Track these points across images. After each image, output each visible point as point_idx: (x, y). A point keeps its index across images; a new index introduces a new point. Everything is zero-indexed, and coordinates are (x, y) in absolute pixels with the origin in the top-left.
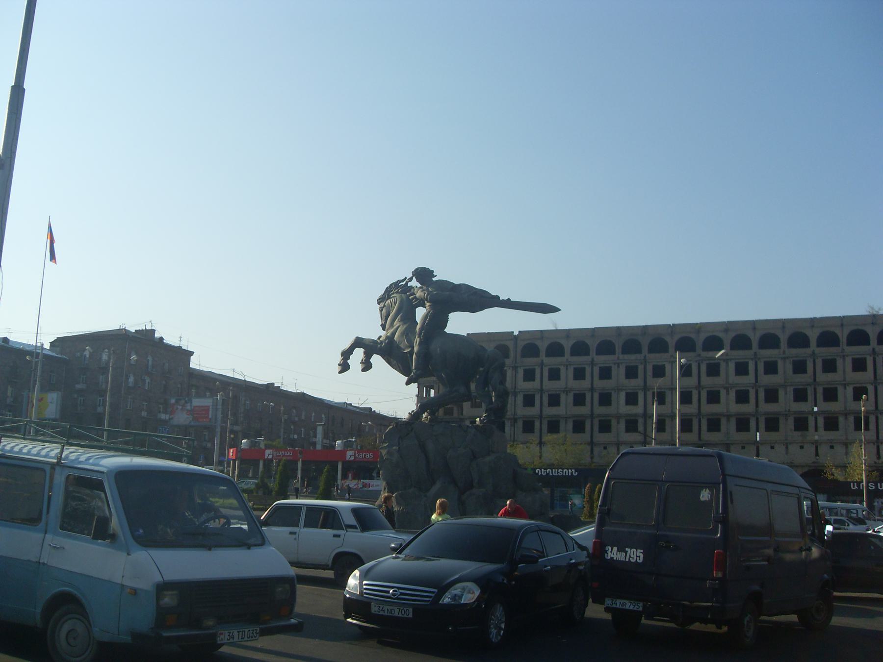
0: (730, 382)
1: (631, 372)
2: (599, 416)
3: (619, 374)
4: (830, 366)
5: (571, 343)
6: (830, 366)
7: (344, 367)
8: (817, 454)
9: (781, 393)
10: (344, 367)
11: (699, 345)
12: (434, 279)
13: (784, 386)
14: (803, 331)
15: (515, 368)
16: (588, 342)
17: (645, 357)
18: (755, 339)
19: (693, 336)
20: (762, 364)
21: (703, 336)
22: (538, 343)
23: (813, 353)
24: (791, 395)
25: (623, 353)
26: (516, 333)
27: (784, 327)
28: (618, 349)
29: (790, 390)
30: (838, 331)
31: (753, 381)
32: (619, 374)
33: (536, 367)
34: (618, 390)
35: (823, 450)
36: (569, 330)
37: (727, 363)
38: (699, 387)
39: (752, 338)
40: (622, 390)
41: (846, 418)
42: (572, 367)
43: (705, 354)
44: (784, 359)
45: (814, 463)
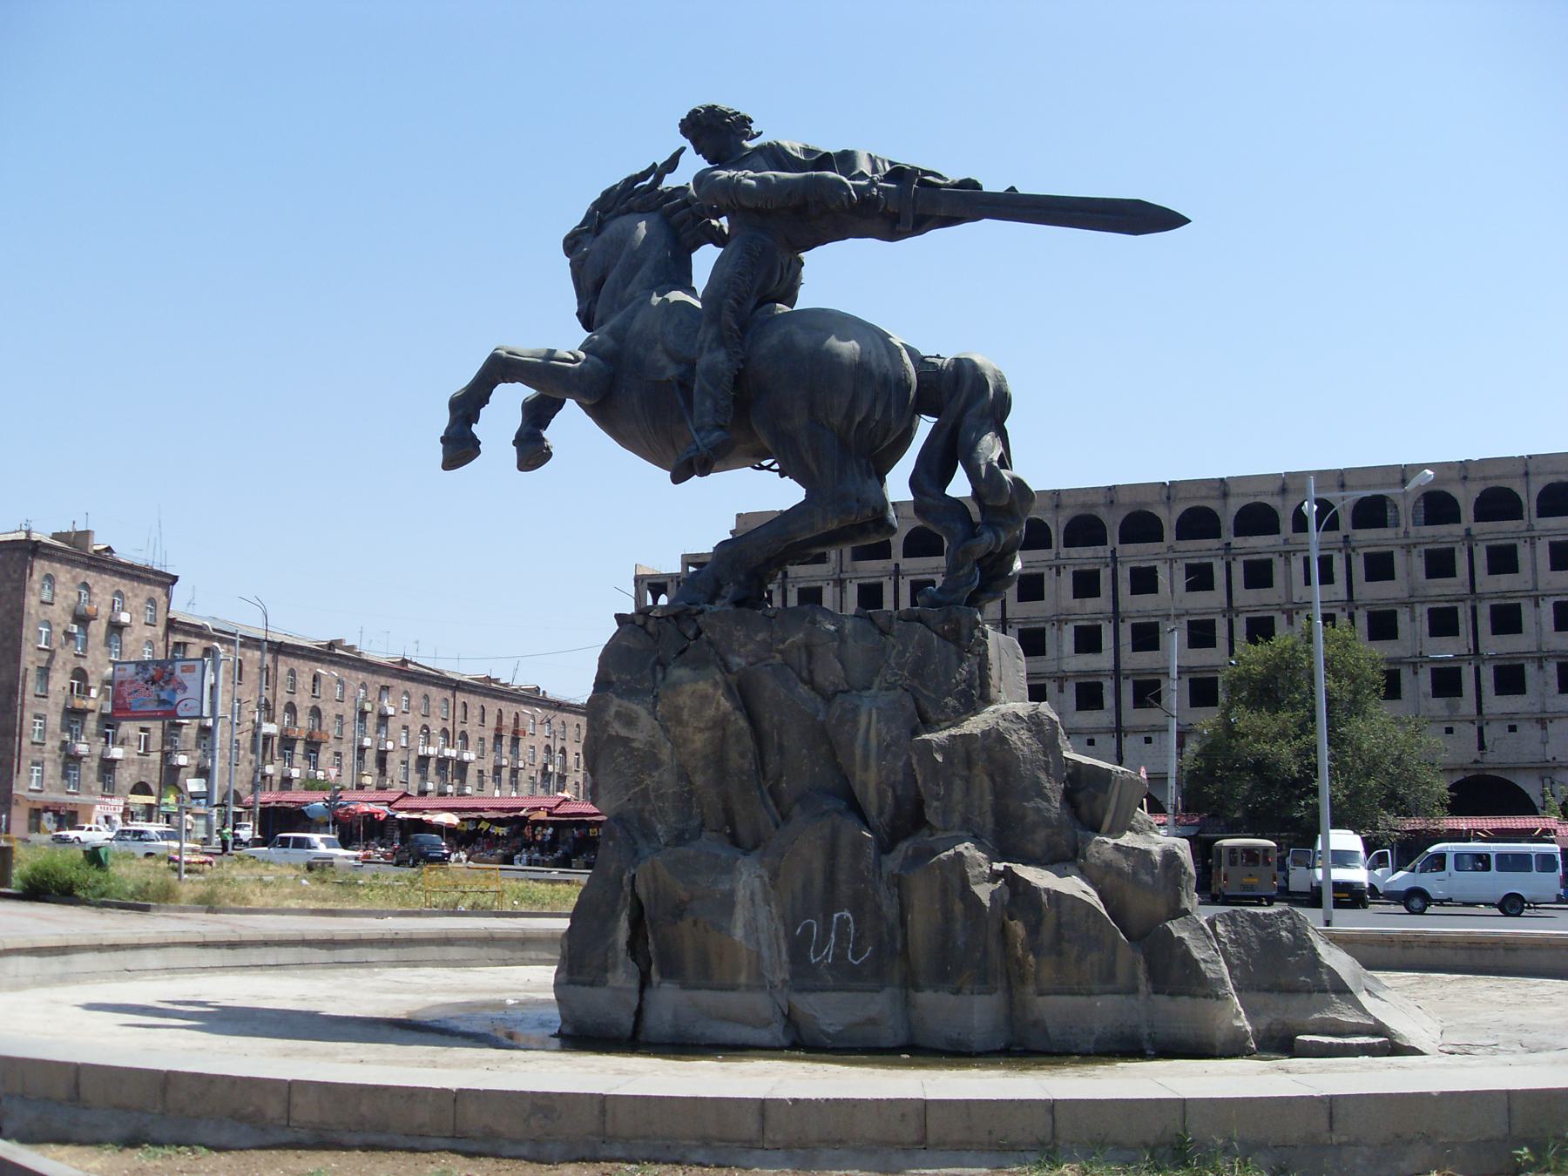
1: (1086, 584)
4: (1503, 560)
6: (1503, 560)
7: (460, 446)
8: (1482, 746)
9: (1403, 618)
10: (460, 446)
11: (1227, 523)
12: (750, 144)
13: (1409, 604)
14: (1447, 489)
15: (840, 583)
17: (1113, 552)
21: (1236, 504)
23: (1468, 531)
24: (1424, 625)
25: (1066, 546)
28: (1057, 537)
29: (1422, 611)
30: (1518, 487)
33: (885, 580)
34: (1060, 621)
35: (1493, 732)
37: (1288, 561)
38: (1230, 609)
41: (1541, 667)
43: (1238, 542)
44: (1408, 548)
45: (1476, 762)
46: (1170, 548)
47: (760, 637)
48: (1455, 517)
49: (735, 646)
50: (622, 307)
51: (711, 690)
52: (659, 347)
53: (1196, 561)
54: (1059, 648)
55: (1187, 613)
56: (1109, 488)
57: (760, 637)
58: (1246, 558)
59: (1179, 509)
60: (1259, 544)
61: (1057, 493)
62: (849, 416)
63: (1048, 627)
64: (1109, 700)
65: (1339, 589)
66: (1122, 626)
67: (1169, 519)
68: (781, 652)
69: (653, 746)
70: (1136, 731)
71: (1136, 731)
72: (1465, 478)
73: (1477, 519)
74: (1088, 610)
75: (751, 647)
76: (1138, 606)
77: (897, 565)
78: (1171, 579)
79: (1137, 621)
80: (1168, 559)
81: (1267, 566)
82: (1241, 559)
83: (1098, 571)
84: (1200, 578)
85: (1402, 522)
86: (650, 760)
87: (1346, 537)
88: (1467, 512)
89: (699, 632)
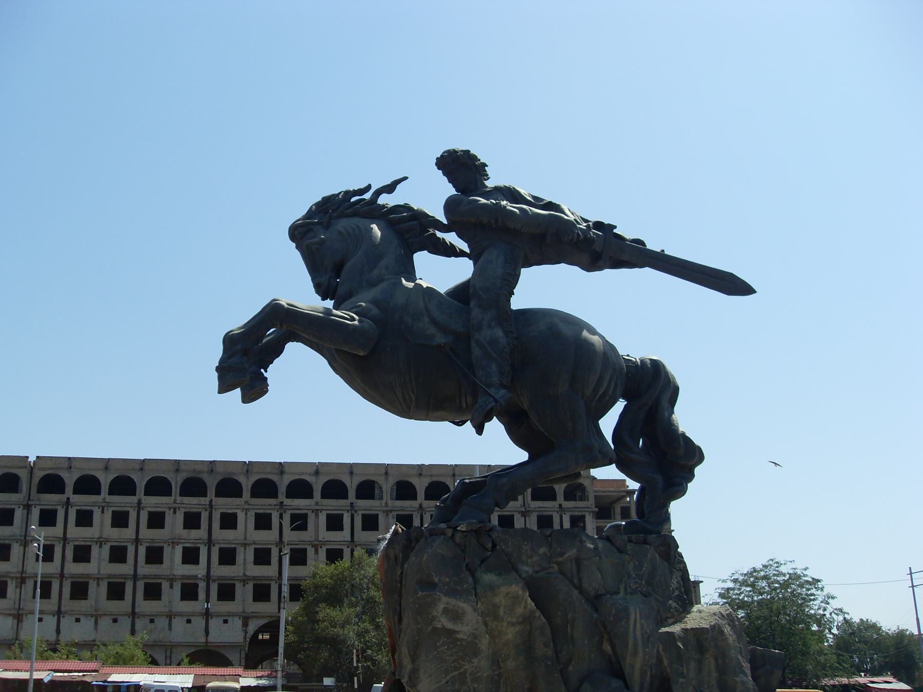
1: (192, 521)
2: (145, 577)
3: (175, 523)
5: (111, 477)
11: (282, 489)
12: (490, 184)
14: (410, 480)
15: (28, 507)
17: (211, 501)
19: (275, 478)
20: (360, 517)
21: (287, 479)
22: (64, 475)
23: (421, 506)
25: (180, 495)
26: (32, 459)
27: (386, 473)
31: (348, 538)
32: (175, 523)
34: (174, 543)
36: (109, 460)
37: (317, 516)
39: (348, 484)
42: (111, 510)
43: (288, 502)
44: (387, 513)
46: (246, 502)
47: (542, 551)
48: (414, 497)
49: (524, 558)
50: (373, 284)
51: (520, 592)
52: (426, 319)
53: (262, 511)
54: (172, 560)
55: (254, 543)
56: (211, 462)
57: (542, 551)
58: (292, 512)
59: (253, 479)
61: (177, 462)
62: (596, 390)
63: (166, 546)
64: (202, 595)
65: (346, 534)
67: (247, 484)
68: (558, 564)
69: (476, 637)
70: (218, 615)
71: (218, 615)
72: (420, 474)
73: (566, 499)
74: (192, 537)
75: (535, 558)
77: (68, 499)
78: (246, 522)
79: (223, 546)
81: (304, 517)
82: (289, 512)
83: (200, 513)
84: (263, 522)
85: (385, 497)
86: (471, 649)
87: (352, 504)
88: (421, 494)
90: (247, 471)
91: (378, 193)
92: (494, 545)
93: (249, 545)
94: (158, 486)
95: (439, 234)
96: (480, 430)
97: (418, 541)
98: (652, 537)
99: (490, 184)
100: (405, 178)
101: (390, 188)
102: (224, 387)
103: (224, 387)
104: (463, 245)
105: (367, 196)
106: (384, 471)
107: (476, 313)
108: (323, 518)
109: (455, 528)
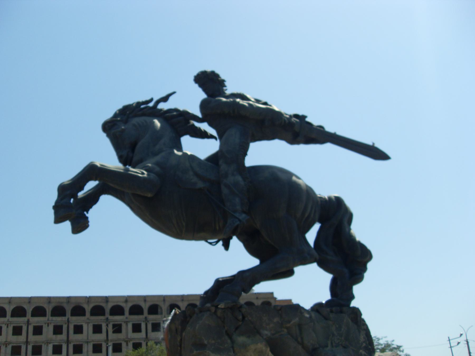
0: (129, 337)
1: (58, 330)
3: (48, 332)
5: (12, 307)
11: (107, 311)
12: (228, 92)
16: (25, 307)
17: (68, 319)
18: (145, 307)
19: (103, 305)
21: (110, 305)
27: (164, 300)
28: (49, 312)
32: (48, 332)
34: (48, 343)
36: (11, 298)
37: (127, 325)
40: (50, 343)
42: (12, 326)
43: (111, 318)
46: (88, 319)
47: (276, 320)
51: (264, 348)
52: (191, 173)
55: (93, 341)
57: (276, 320)
59: (92, 305)
60: (118, 319)
63: (43, 345)
65: (143, 334)
66: (70, 345)
67: (88, 309)
68: (287, 328)
75: (272, 325)
76: (76, 338)
78: (88, 329)
79: (75, 343)
80: (87, 322)
84: (97, 329)
87: (146, 318)
89: (244, 318)
90: (88, 302)
91: (158, 102)
92: (244, 318)
93: (90, 342)
94: (39, 311)
95: (197, 124)
96: (226, 246)
97: (191, 317)
98: (345, 309)
99: (228, 92)
100: (174, 93)
101: (165, 99)
102: (58, 219)
103: (58, 219)
104: (213, 132)
105: (151, 105)
106: (162, 299)
107: (223, 167)
108: (130, 326)
109: (216, 307)
